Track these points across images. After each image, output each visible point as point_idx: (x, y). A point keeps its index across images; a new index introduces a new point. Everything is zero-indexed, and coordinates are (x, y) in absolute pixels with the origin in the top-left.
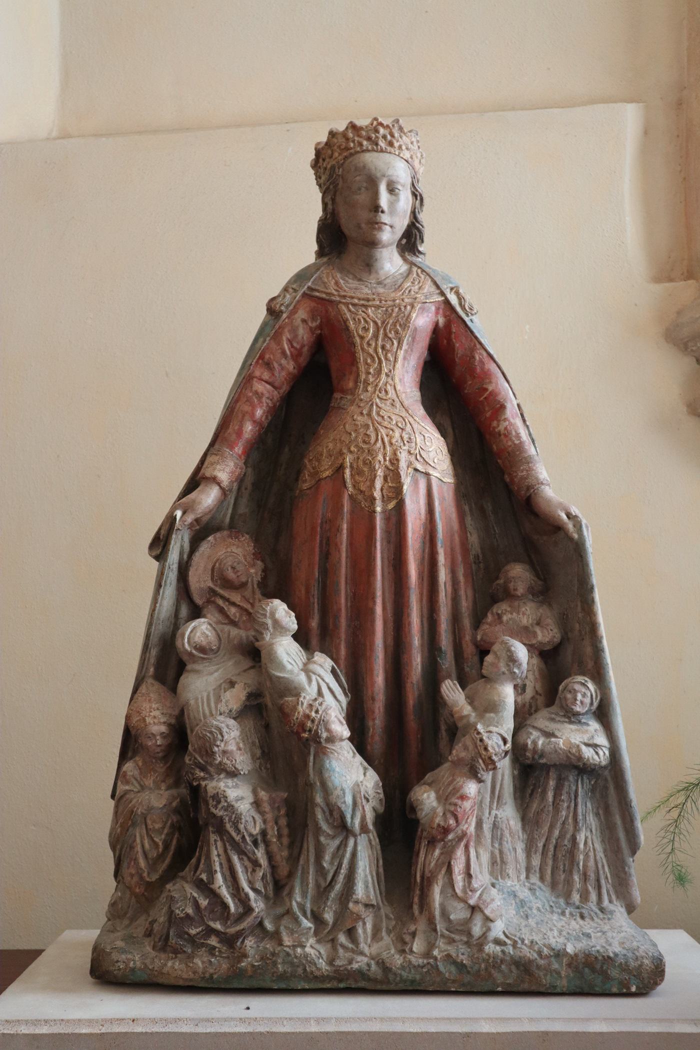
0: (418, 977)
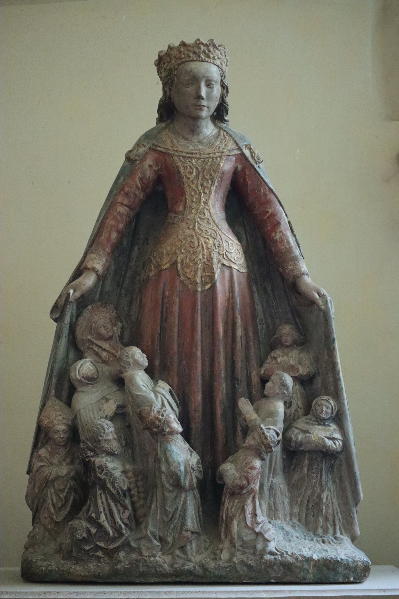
0: (224, 574)
